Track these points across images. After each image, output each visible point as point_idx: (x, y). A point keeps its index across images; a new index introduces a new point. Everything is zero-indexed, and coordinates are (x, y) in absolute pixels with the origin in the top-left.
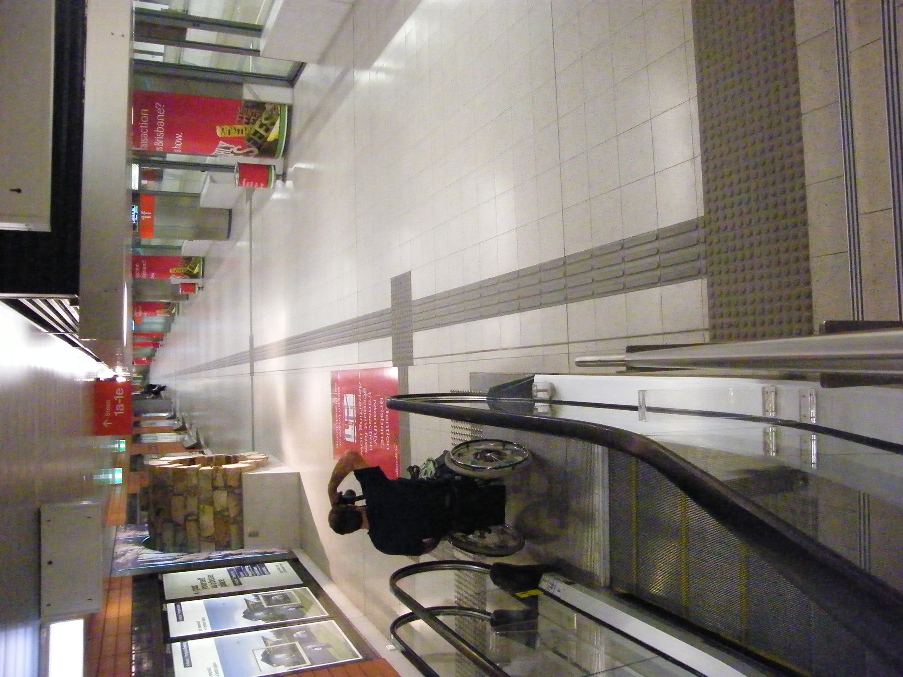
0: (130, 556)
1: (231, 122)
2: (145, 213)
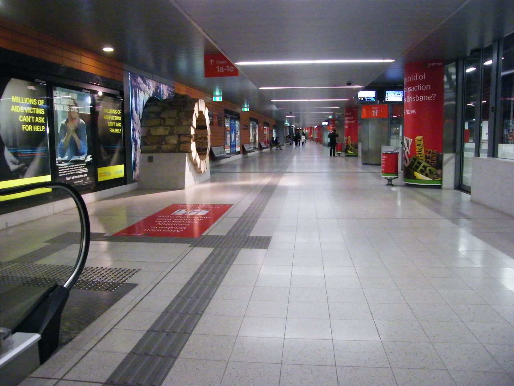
0: (143, 86)
1: (426, 146)
2: (376, 112)
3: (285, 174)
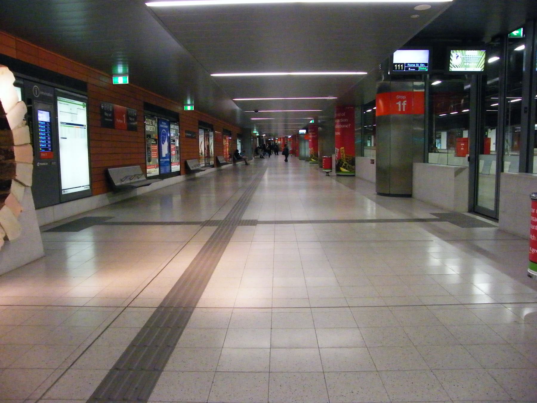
2: (404, 104)
3: (240, 230)
